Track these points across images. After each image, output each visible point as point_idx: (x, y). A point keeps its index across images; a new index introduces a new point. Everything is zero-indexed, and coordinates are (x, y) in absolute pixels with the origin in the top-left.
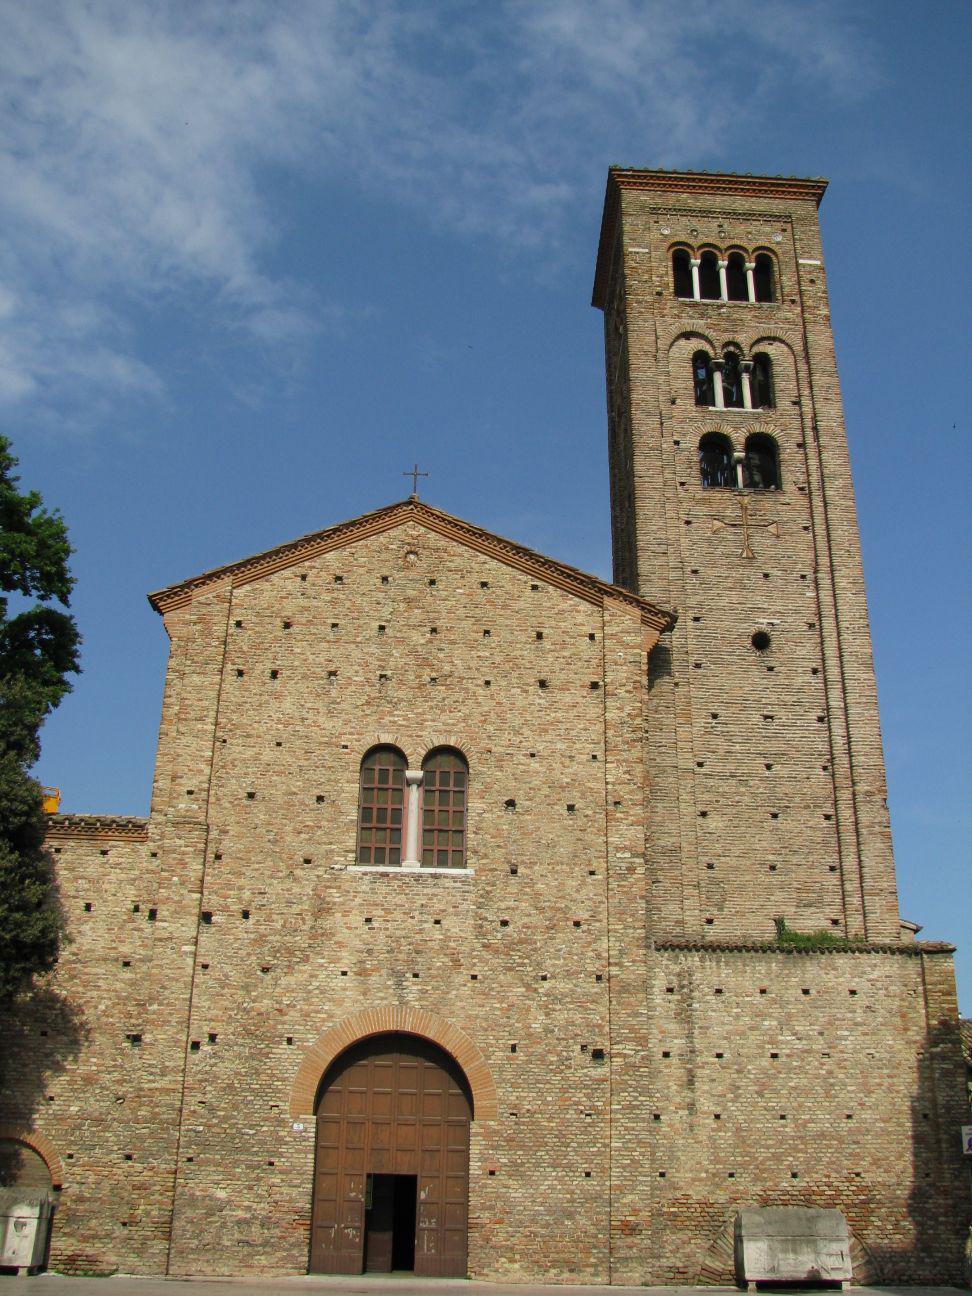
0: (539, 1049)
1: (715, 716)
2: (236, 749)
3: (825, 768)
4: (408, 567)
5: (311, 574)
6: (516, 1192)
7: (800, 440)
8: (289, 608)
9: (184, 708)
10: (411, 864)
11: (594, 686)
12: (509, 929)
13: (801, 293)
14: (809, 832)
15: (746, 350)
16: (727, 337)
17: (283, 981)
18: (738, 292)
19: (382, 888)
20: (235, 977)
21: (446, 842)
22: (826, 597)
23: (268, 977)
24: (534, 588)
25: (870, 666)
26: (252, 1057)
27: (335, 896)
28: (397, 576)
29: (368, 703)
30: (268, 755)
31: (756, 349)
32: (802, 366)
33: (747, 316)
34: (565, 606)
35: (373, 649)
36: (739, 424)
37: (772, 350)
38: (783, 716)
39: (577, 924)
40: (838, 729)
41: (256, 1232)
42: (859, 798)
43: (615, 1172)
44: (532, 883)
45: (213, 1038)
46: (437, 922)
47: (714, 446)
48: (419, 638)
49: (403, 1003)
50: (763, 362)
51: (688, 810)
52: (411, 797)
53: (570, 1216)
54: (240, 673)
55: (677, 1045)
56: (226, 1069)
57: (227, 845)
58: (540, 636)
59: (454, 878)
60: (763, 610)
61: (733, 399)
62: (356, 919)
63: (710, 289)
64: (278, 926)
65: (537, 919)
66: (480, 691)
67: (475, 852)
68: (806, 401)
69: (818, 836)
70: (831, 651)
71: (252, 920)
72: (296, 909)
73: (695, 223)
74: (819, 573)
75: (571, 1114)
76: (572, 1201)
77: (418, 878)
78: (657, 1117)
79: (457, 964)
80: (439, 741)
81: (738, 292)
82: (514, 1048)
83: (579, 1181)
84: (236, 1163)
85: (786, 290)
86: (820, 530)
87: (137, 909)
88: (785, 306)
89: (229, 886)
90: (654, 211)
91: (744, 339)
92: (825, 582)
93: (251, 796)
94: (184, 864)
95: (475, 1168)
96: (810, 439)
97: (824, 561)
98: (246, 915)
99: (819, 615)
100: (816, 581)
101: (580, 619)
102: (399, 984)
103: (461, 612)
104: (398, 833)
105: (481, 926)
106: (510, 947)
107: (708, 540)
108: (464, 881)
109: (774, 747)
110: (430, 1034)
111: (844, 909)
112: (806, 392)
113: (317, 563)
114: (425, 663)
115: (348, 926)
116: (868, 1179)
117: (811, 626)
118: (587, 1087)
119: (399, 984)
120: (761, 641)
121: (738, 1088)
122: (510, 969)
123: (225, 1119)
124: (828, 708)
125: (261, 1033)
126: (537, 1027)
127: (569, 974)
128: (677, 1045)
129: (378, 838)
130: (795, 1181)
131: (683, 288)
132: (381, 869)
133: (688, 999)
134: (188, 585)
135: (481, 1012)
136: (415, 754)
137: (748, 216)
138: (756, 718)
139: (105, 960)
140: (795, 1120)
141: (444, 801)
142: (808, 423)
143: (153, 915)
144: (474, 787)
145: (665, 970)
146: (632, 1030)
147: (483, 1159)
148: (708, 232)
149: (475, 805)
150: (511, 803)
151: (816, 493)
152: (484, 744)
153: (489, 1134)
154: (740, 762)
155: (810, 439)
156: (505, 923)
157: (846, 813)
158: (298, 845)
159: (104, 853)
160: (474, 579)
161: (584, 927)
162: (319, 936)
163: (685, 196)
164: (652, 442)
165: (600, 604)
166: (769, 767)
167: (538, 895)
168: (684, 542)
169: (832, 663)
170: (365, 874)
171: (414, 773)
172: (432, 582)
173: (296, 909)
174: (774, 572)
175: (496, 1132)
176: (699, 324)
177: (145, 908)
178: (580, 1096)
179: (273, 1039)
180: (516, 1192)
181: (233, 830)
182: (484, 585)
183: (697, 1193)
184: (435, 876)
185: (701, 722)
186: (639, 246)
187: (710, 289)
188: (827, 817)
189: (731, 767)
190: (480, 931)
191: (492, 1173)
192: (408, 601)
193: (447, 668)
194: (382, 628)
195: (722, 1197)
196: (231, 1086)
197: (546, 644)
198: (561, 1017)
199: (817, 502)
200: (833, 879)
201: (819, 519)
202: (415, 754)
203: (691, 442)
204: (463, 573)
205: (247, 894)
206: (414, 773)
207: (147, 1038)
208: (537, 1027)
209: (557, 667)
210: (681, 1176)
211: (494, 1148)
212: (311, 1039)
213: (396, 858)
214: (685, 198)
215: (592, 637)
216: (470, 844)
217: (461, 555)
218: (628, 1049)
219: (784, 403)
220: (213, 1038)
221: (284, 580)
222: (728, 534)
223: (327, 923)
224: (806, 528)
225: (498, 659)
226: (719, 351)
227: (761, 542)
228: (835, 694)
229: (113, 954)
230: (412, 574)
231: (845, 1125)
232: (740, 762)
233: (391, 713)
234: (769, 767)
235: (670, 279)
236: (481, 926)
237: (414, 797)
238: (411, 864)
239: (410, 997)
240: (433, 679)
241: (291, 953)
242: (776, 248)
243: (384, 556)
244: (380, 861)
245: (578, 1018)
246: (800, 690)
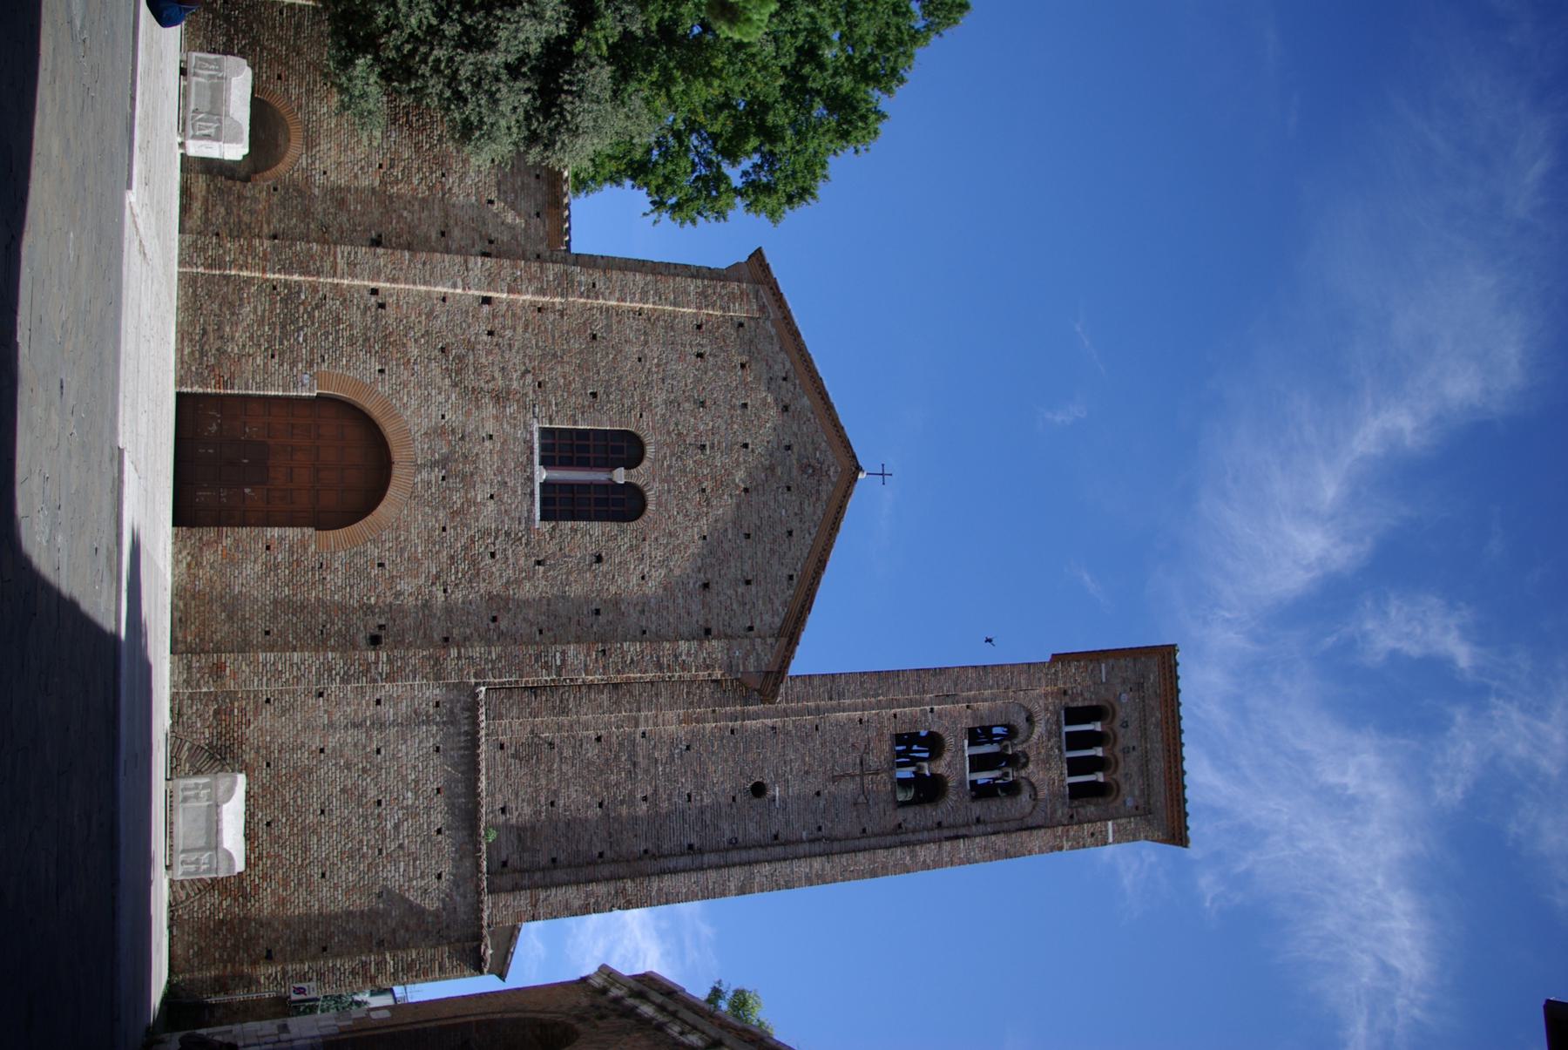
1: (688, 748)
3: (646, 851)
4: (803, 469)
5: (790, 386)
7: (945, 823)
10: (541, 474)
11: (708, 632)
12: (488, 561)
13: (1080, 823)
14: (587, 837)
15: (1023, 773)
16: (1032, 754)
23: (437, 352)
24: (791, 577)
26: (367, 339)
27: (512, 409)
29: (679, 434)
30: (633, 350)
31: (1024, 783)
32: (1013, 825)
33: (1054, 774)
34: (777, 603)
37: (1025, 797)
39: (494, 619)
42: (620, 884)
43: (271, 656)
44: (528, 578)
45: (382, 306)
46: (492, 497)
47: (934, 744)
49: (419, 468)
50: (1012, 789)
53: (230, 618)
54: (699, 327)
55: (388, 712)
58: (748, 582)
59: (530, 511)
61: (978, 763)
62: (490, 427)
63: (1075, 741)
64: (483, 360)
67: (554, 528)
68: (981, 828)
69: (583, 847)
70: (752, 854)
71: (485, 338)
72: (497, 374)
75: (322, 617)
76: (244, 619)
77: (531, 479)
78: (321, 695)
79: (455, 514)
80: (651, 496)
81: (1075, 767)
82: (381, 565)
83: (262, 626)
84: (272, 326)
85: (1081, 810)
86: (864, 842)
87: (491, 242)
88: (1066, 810)
90: (1140, 686)
92: (817, 848)
93: (594, 337)
96: (946, 833)
97: (836, 846)
98: (490, 333)
99: (787, 843)
100: (819, 840)
101: (766, 617)
102: (434, 464)
105: (489, 534)
107: (846, 740)
108: (530, 519)
110: (391, 491)
111: (515, 870)
115: (487, 418)
117: (776, 837)
118: (348, 630)
119: (434, 464)
121: (349, 769)
122: (452, 557)
123: (311, 316)
124: (701, 851)
126: (402, 586)
129: (562, 447)
130: (263, 825)
131: (1074, 715)
132: (536, 446)
135: (413, 536)
139: (447, 216)
140: (320, 823)
142: (963, 831)
143: (485, 254)
144: (612, 527)
146: (401, 669)
147: (281, 539)
148: (1127, 738)
149: (597, 528)
150: (599, 559)
151: (897, 839)
154: (647, 771)
156: (493, 555)
158: (555, 374)
159: (538, 215)
160: (795, 524)
161: (492, 626)
163: (1158, 714)
165: (779, 634)
166: (645, 799)
167: (519, 582)
169: (744, 855)
170: (532, 434)
171: (620, 476)
172: (789, 489)
173: (497, 374)
175: (306, 549)
176: (1039, 729)
179: (384, 360)
182: (790, 533)
184: (532, 494)
186: (1108, 673)
187: (1075, 741)
188: (601, 855)
190: (486, 533)
191: (268, 548)
192: (772, 468)
194: (746, 446)
196: (338, 320)
199: (889, 840)
200: (543, 859)
202: (639, 475)
204: (800, 514)
206: (620, 476)
207: (380, 251)
209: (722, 598)
210: (266, 718)
211: (291, 547)
212: (384, 389)
215: (751, 628)
216: (562, 524)
218: (384, 668)
219: (977, 809)
220: (382, 306)
222: (854, 757)
224: (864, 830)
225: (726, 546)
226: (1019, 748)
229: (452, 222)
230: (795, 472)
231: (316, 871)
232: (647, 771)
233: (673, 454)
234: (645, 799)
235: (1079, 703)
236: (489, 534)
237: (599, 476)
238: (541, 474)
239: (424, 474)
240: (704, 490)
242: (1119, 801)
243: (810, 448)
244: (543, 448)
245: (409, 622)
246: (717, 827)
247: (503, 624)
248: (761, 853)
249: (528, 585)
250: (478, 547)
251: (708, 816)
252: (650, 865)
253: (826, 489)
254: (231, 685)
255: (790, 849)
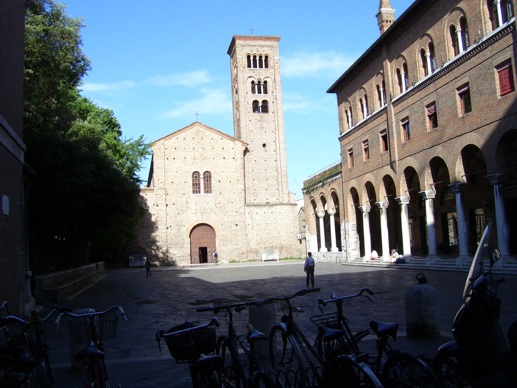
0: (227, 225)
2: (168, 174)
6: (224, 249)
8: (175, 146)
9: (158, 166)
17: (182, 216)
18: (261, 66)
19: (197, 198)
20: (173, 216)
21: (208, 190)
22: (277, 136)
25: (285, 150)
27: (189, 200)
28: (195, 137)
30: (175, 174)
32: (274, 84)
35: (192, 153)
36: (260, 98)
38: (268, 160)
40: (279, 163)
41: (182, 258)
47: (255, 102)
48: (201, 150)
50: (265, 82)
51: (251, 180)
52: (202, 182)
56: (173, 232)
57: (169, 192)
60: (265, 139)
61: (259, 92)
62: (194, 204)
63: (255, 66)
65: (226, 202)
66: (213, 160)
69: (275, 183)
70: (278, 147)
73: (252, 48)
74: (276, 130)
83: (234, 246)
89: (170, 199)
90: (243, 46)
91: (262, 78)
92: (277, 133)
94: (162, 196)
95: (217, 245)
97: (277, 128)
101: (231, 145)
103: (208, 145)
104: (199, 188)
106: (221, 207)
109: (267, 166)
112: (274, 90)
113: (180, 135)
114: (202, 155)
116: (282, 243)
120: (264, 145)
125: (179, 226)
126: (226, 221)
127: (231, 212)
128: (250, 223)
129: (196, 189)
131: (249, 66)
133: (252, 215)
134: (156, 141)
136: (202, 173)
137: (263, 46)
138: (263, 161)
141: (207, 181)
142: (275, 98)
145: (248, 209)
152: (214, 170)
153: (219, 239)
155: (275, 101)
157: (280, 179)
160: (210, 138)
162: (187, 207)
164: (243, 104)
168: (250, 125)
169: (278, 149)
171: (202, 176)
174: (267, 131)
176: (252, 75)
177: (156, 205)
178: (234, 232)
179: (181, 226)
180: (224, 249)
181: (170, 189)
183: (254, 247)
185: (253, 162)
187: (255, 66)
189: (259, 171)
193: (206, 156)
195: (258, 248)
197: (224, 150)
198: (230, 219)
199: (276, 116)
201: (276, 119)
202: (202, 173)
203: (251, 102)
205: (174, 201)
206: (202, 176)
208: (226, 221)
213: (199, 192)
214: (250, 42)
217: (208, 133)
218: (242, 224)
221: (173, 139)
222: (258, 123)
223: (189, 205)
225: (216, 154)
227: (265, 124)
228: (278, 156)
241: (183, 211)
244: (197, 193)
245: (233, 219)
246: (272, 155)
247: (233, 201)
248: (278, 145)
249: (226, 196)
250: (218, 206)
251: (270, 157)
252: (279, 171)
253: (202, 129)
254: (246, 251)
255: (277, 139)
